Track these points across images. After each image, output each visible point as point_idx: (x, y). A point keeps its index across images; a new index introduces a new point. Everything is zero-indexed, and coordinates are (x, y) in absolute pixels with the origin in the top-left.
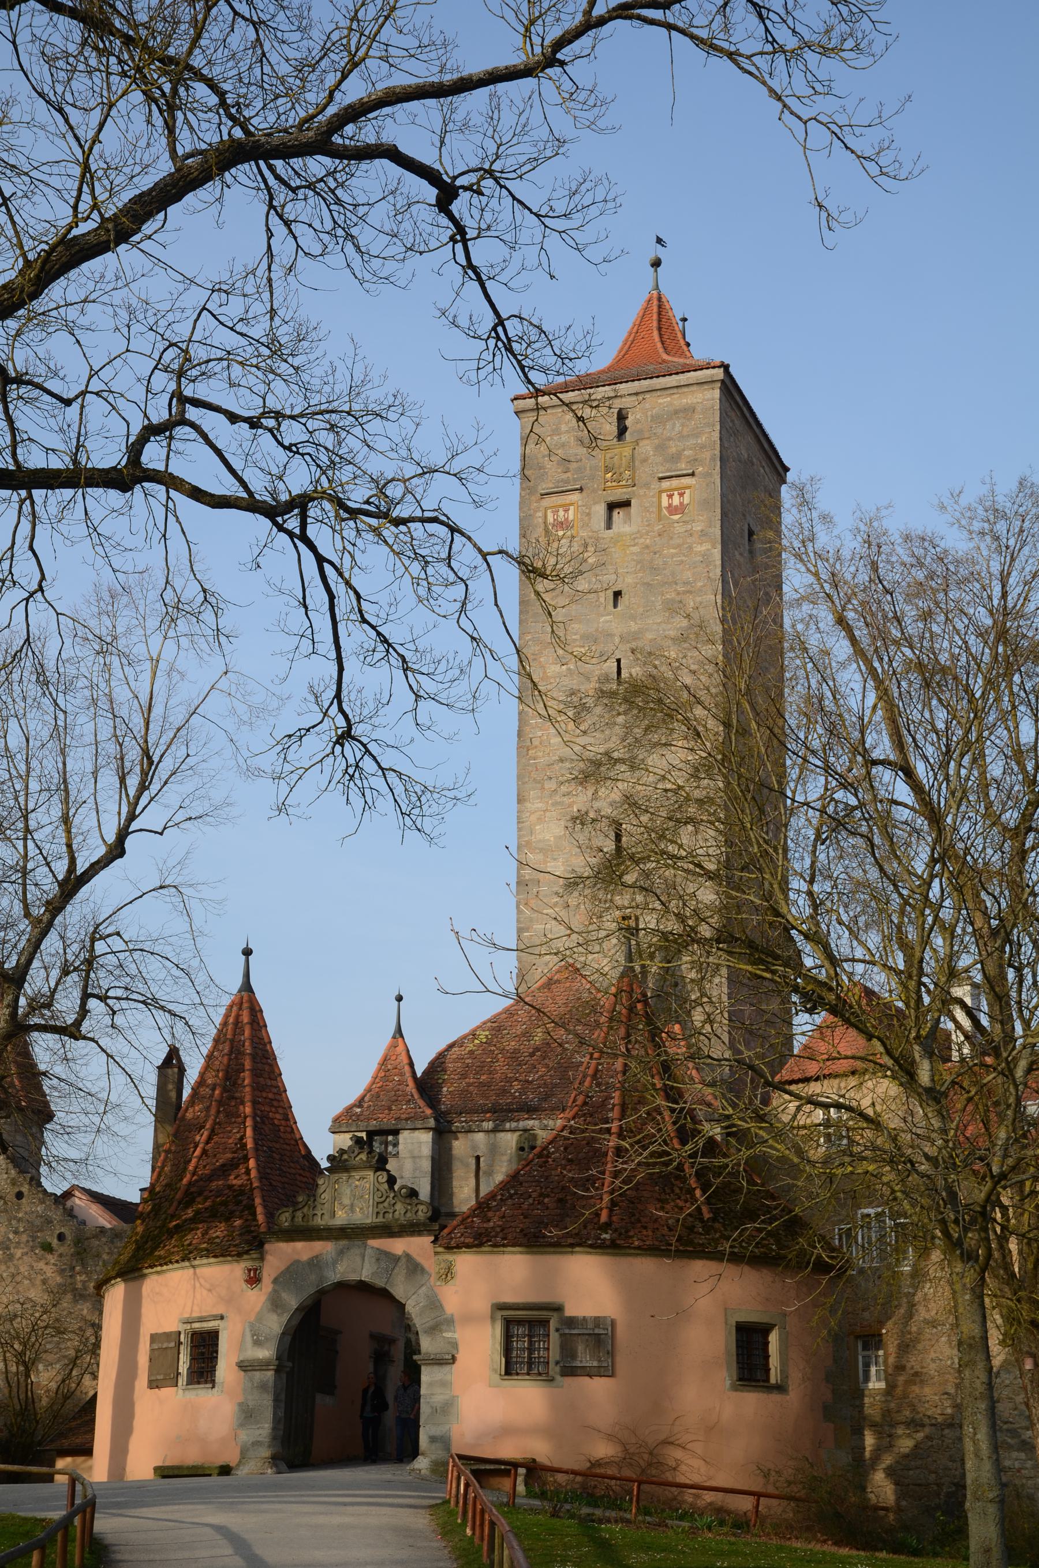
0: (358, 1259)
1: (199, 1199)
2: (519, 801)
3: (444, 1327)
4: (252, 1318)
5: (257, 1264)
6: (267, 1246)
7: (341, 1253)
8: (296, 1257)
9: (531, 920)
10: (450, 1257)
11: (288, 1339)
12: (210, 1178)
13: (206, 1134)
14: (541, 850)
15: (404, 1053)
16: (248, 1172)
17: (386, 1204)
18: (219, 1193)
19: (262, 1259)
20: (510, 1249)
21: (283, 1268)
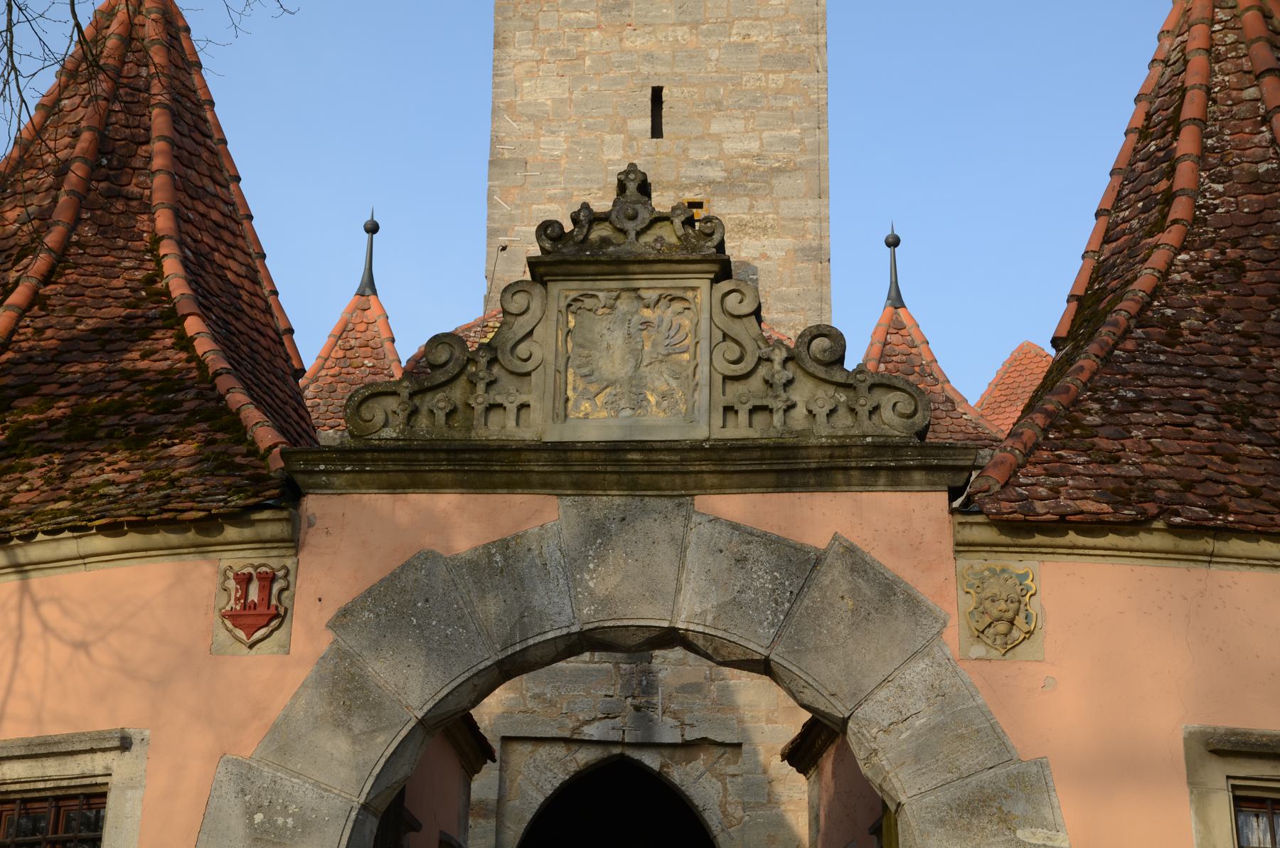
0: (665, 553)
1: (24, 403)
2: (497, 45)
3: (1019, 809)
4: (249, 745)
5: (273, 560)
6: (312, 504)
7: (598, 534)
8: (430, 542)
9: (512, 218)
10: (1017, 564)
11: (372, 824)
12: (60, 356)
13: (40, 263)
14: (531, 118)
15: (381, 321)
16: (185, 343)
17: (756, 383)
18: (90, 386)
19: (293, 543)
20: (1237, 546)
21: (374, 574)
